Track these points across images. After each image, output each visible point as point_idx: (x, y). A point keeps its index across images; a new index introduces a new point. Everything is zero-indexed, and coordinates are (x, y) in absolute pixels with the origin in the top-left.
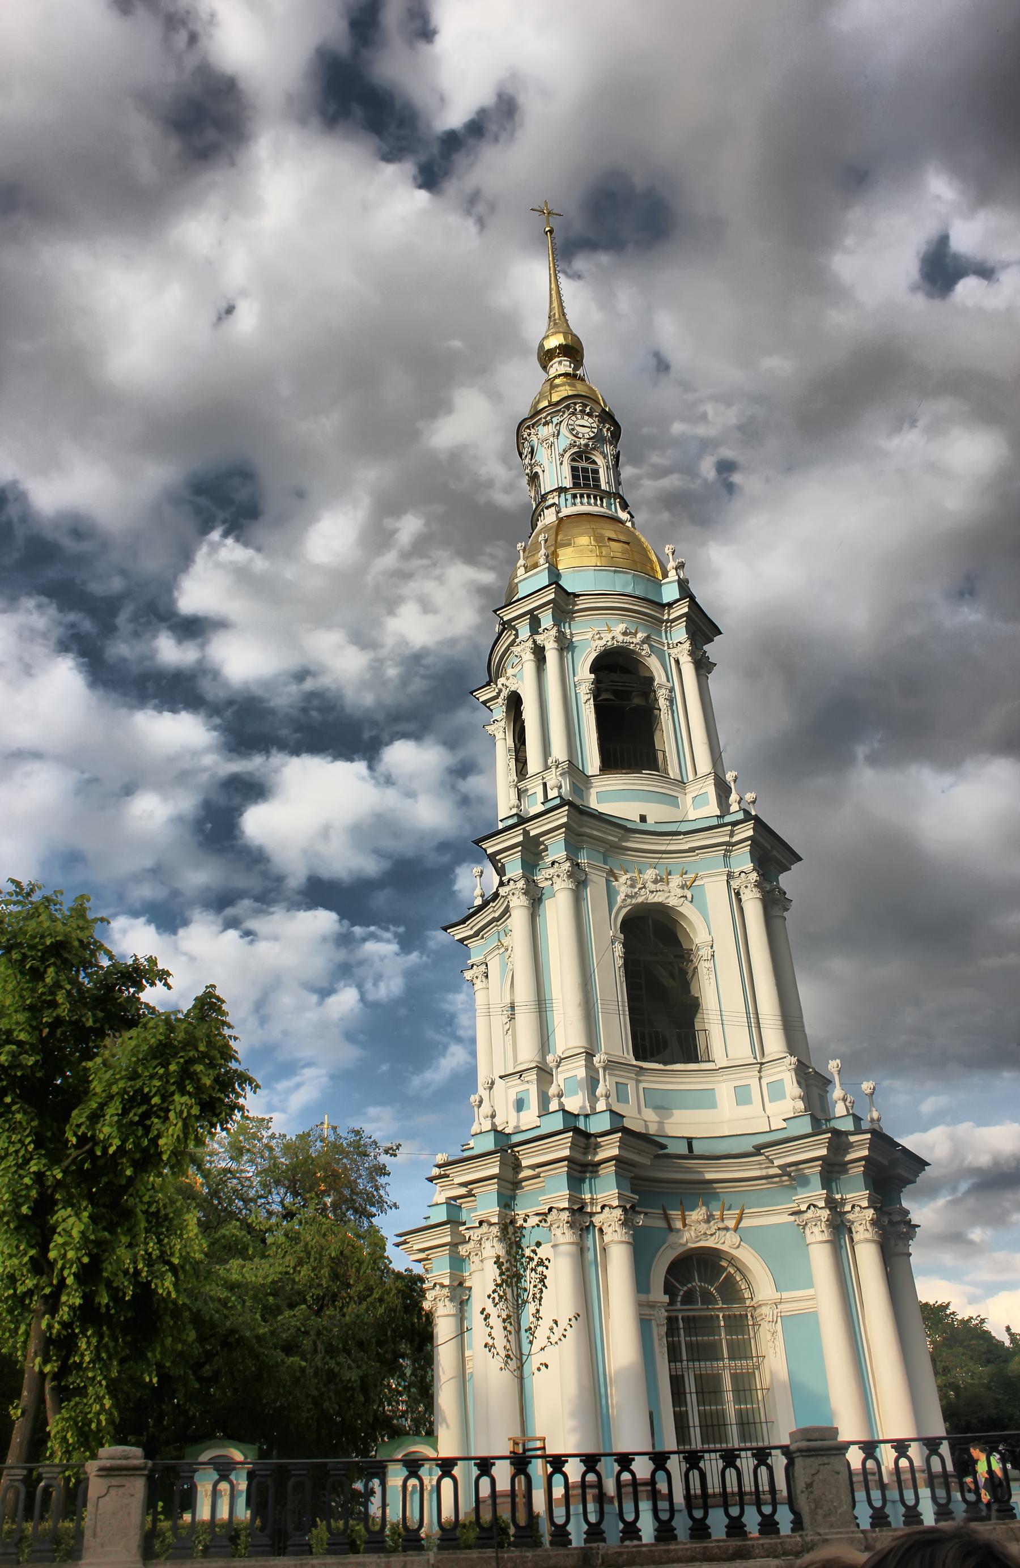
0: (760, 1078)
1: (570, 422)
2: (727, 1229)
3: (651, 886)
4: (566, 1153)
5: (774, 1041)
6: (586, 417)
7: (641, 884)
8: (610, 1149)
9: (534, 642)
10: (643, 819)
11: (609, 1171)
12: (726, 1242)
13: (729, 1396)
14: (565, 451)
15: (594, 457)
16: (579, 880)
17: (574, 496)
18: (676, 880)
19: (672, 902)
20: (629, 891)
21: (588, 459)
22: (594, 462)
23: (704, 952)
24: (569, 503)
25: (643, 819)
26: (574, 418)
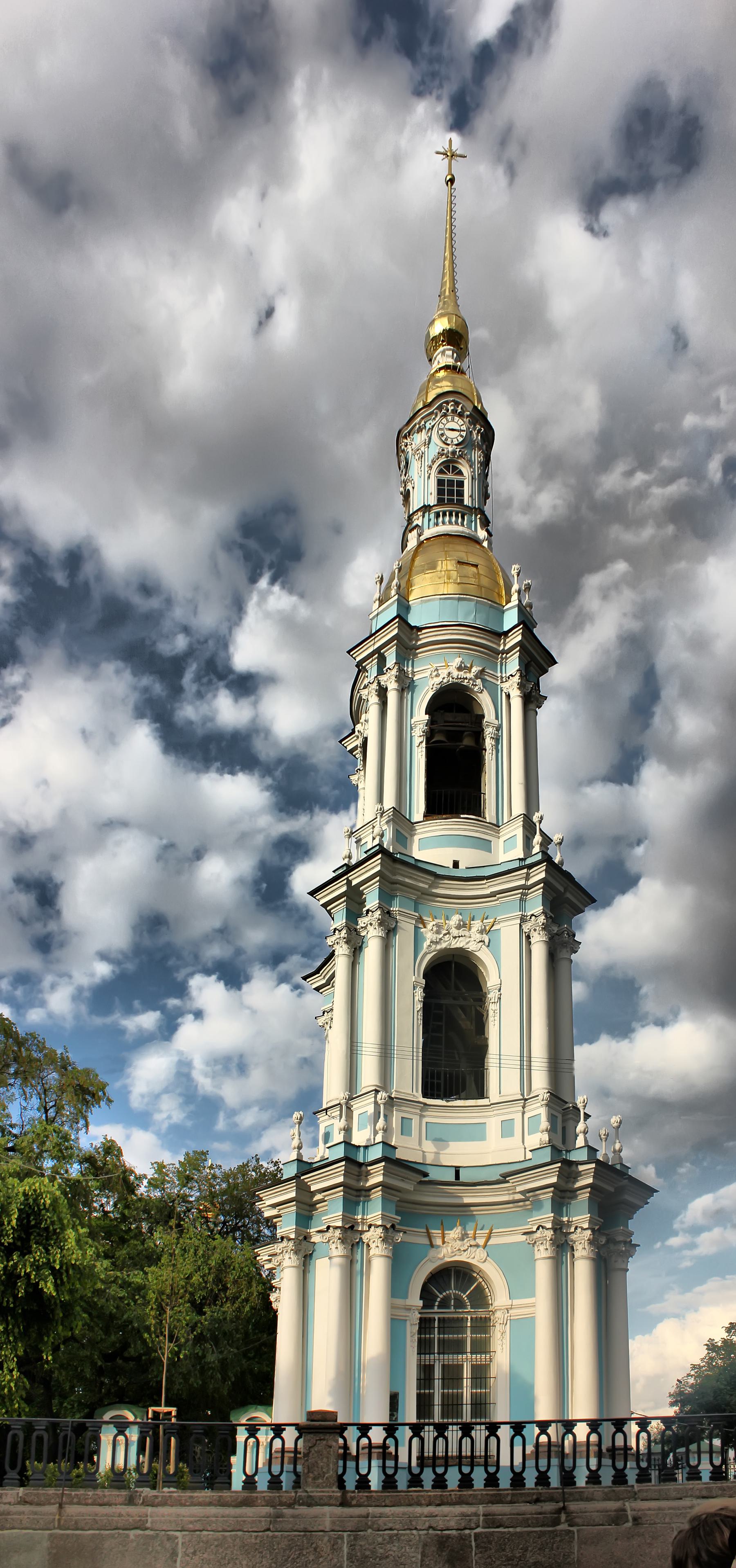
0: (523, 1113)
1: (441, 426)
2: (477, 1246)
3: (455, 932)
4: (341, 1179)
5: (540, 1081)
6: (456, 418)
7: (444, 932)
8: (376, 1177)
9: (379, 683)
10: (456, 864)
11: (377, 1194)
12: (474, 1257)
13: (467, 1383)
14: (433, 462)
15: (460, 467)
16: (389, 929)
17: (437, 515)
18: (477, 925)
19: (472, 947)
20: (435, 937)
21: (454, 468)
22: (460, 473)
23: (492, 996)
24: (432, 523)
25: (456, 864)
26: (444, 421)
